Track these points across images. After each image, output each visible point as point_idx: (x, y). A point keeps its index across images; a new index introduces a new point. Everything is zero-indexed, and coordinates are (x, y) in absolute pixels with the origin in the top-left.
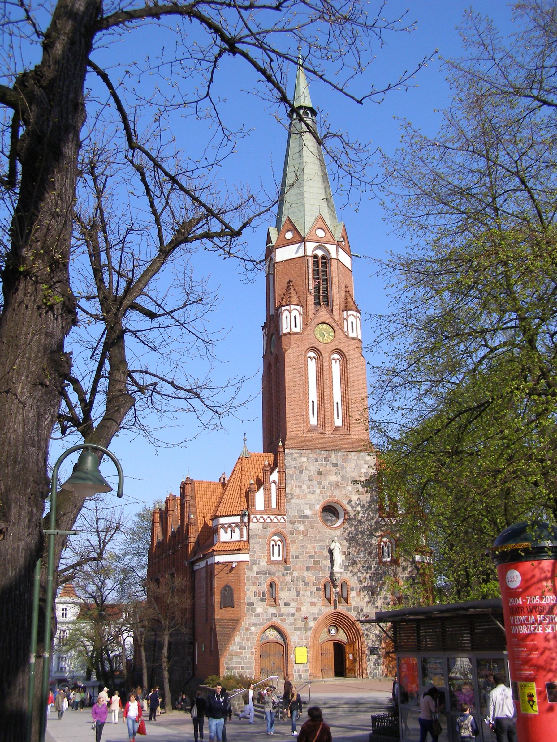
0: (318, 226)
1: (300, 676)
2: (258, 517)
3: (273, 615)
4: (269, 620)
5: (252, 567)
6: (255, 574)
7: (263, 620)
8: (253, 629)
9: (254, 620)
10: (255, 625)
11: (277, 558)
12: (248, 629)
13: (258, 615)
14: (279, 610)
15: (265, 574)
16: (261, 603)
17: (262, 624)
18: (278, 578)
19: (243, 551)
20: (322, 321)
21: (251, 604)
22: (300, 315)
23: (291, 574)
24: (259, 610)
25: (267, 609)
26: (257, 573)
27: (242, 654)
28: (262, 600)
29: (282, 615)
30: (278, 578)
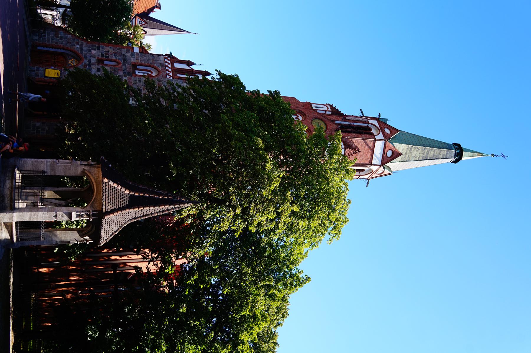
0: (391, 129)
1: (34, 71)
2: (169, 62)
3: (90, 61)
4: (86, 57)
5: (129, 53)
6: (123, 53)
7: (86, 54)
8: (78, 46)
9: (85, 48)
10: (81, 49)
11: (137, 73)
12: (77, 44)
13: (89, 51)
14: (93, 64)
15: (125, 60)
16: (99, 54)
17: (82, 52)
18: (121, 67)
19: (141, 49)
20: (327, 123)
21: (98, 48)
22: (326, 111)
23: (125, 76)
24: (94, 52)
25: (94, 57)
26: (124, 55)
27: (57, 37)
28: (102, 55)
29: (89, 65)
30: (121, 67)
